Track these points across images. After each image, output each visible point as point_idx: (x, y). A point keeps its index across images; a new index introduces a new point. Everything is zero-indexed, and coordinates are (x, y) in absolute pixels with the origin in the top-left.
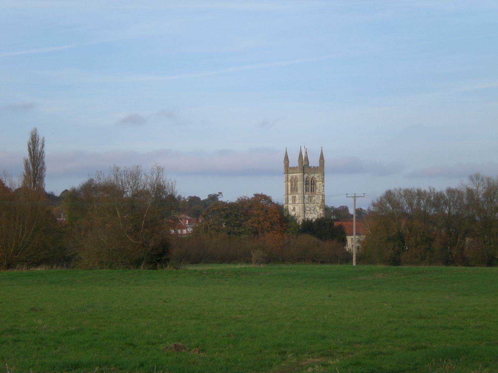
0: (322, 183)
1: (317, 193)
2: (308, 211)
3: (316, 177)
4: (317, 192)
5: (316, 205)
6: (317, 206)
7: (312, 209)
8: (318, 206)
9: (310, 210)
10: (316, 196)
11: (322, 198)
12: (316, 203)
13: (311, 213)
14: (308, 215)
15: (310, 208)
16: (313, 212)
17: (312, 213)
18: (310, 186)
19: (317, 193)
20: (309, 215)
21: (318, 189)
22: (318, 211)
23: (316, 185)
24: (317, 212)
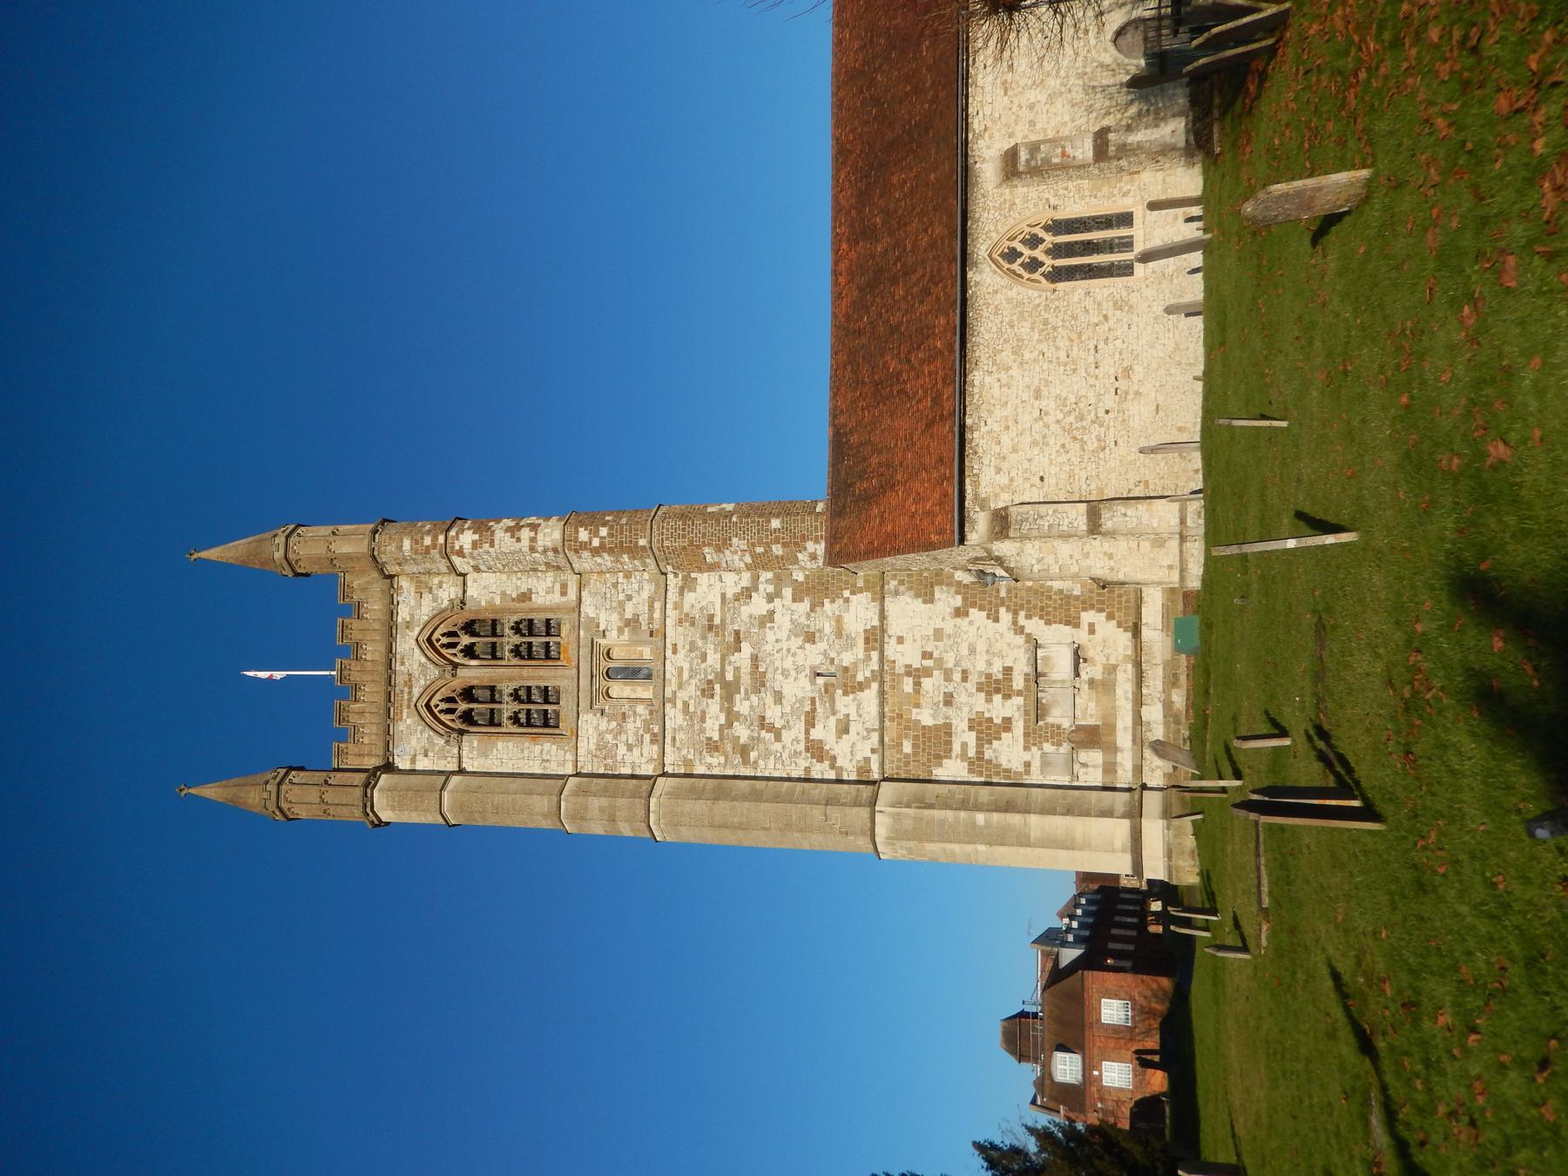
0: (461, 553)
1: (564, 593)
2: (731, 717)
3: (426, 610)
4: (556, 598)
5: (672, 615)
6: (690, 597)
7: (713, 659)
8: (688, 585)
9: (730, 690)
10: (588, 609)
11: (596, 552)
12: (657, 615)
13: (759, 682)
14: (773, 714)
15: (707, 692)
16: (746, 649)
17: (755, 659)
18: (508, 675)
19: (564, 593)
20: (779, 698)
21: (525, 583)
22: (733, 583)
23: (490, 603)
24: (747, 594)
